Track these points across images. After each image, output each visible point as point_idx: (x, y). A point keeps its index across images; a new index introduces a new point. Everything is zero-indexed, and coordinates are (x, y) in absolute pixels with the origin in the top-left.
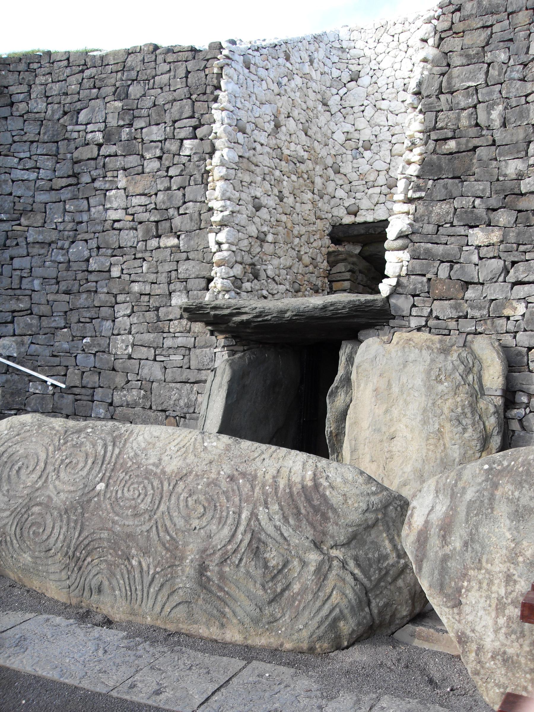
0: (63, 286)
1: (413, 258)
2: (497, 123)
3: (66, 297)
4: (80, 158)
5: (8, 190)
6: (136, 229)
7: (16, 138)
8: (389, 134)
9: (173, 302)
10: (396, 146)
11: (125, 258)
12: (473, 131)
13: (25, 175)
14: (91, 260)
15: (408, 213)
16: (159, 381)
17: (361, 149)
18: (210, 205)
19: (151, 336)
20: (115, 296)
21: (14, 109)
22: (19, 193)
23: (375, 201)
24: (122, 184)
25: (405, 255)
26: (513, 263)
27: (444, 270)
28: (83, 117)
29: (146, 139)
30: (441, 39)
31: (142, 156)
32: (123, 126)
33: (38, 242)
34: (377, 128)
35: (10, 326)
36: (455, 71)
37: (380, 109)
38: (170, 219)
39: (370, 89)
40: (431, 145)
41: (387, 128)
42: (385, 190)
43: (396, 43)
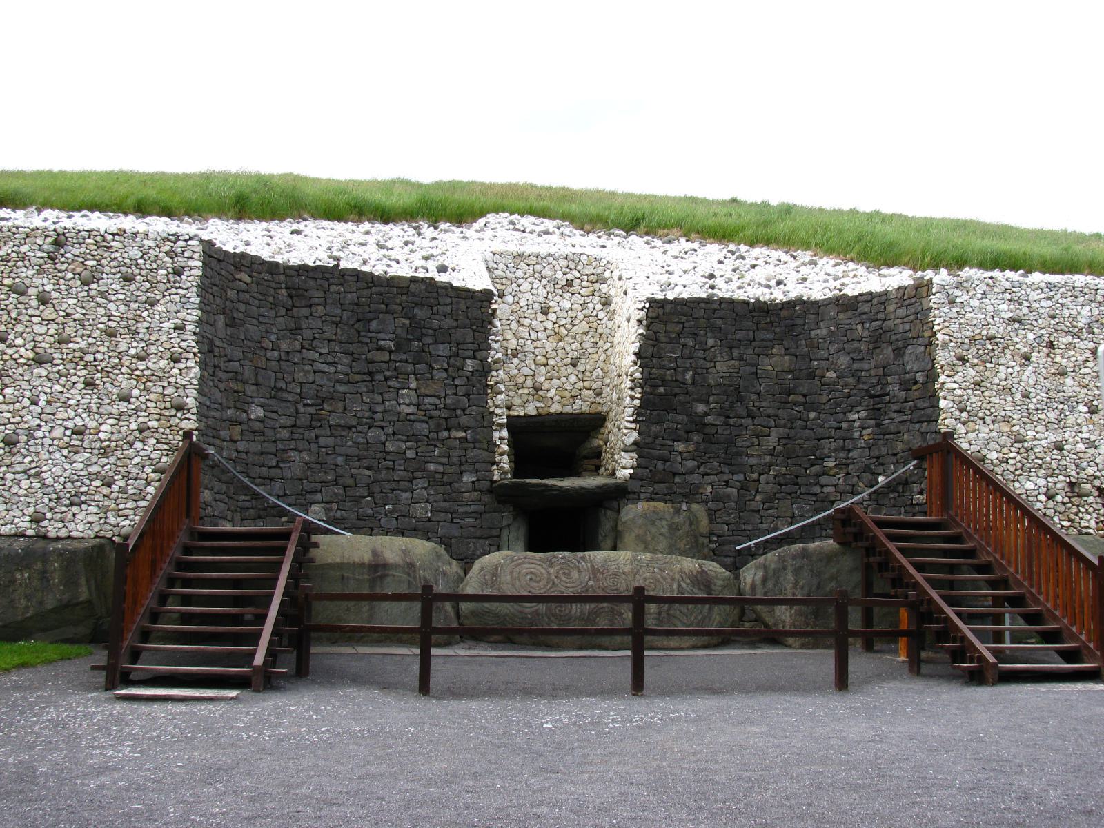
0: (365, 462)
1: (639, 456)
2: (689, 382)
3: (368, 472)
4: (375, 359)
5: (311, 379)
6: (427, 423)
7: (316, 335)
8: (532, 347)
9: (465, 479)
10: (539, 358)
11: (419, 444)
12: (674, 384)
13: (326, 368)
14: (387, 444)
15: (635, 429)
16: (456, 537)
17: (510, 356)
18: (491, 410)
19: (446, 505)
20: (412, 473)
21: (314, 309)
22: (322, 383)
23: (525, 399)
24: (413, 385)
25: (634, 455)
26: (702, 463)
27: (660, 465)
28: (374, 324)
29: (433, 352)
30: (651, 323)
31: (430, 366)
32: (410, 340)
33: (340, 426)
34: (521, 340)
35: (319, 495)
36: (663, 345)
37: (523, 325)
38: (457, 417)
39: (513, 307)
40: (648, 389)
41: (529, 342)
42: (533, 392)
43: (532, 272)
